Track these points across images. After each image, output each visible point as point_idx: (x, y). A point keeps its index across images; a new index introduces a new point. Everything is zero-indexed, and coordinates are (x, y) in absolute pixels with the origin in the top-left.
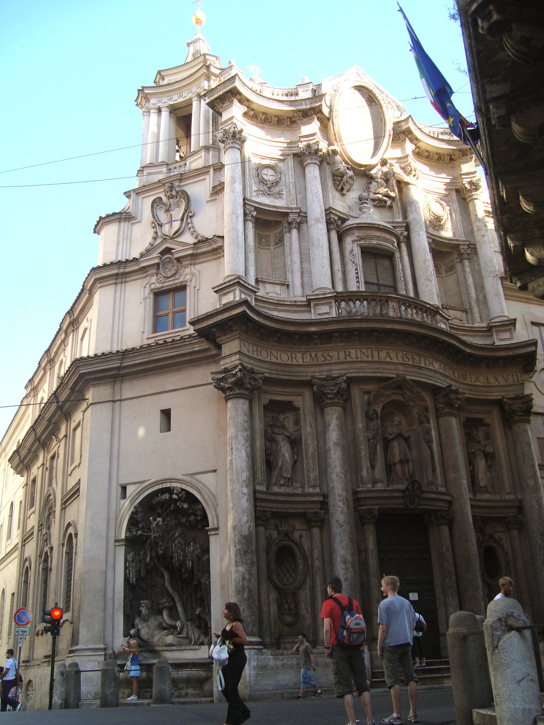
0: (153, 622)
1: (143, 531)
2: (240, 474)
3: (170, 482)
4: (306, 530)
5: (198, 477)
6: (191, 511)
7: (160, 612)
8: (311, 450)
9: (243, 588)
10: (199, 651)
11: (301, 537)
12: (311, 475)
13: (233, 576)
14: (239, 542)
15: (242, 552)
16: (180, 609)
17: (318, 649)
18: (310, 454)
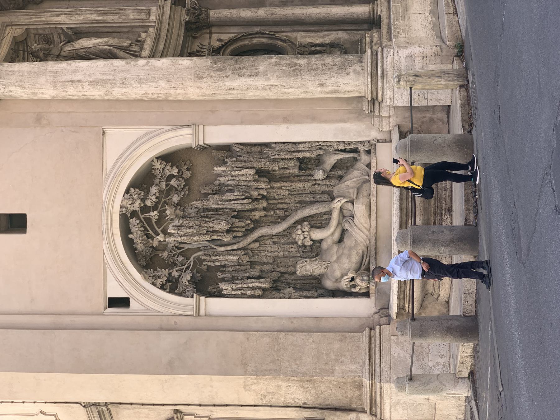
2: (116, 68)
4: (211, 34)
8: (94, 17)
9: (291, 65)
11: (220, 40)
12: (131, 17)
13: (273, 82)
14: (221, 70)
15: (237, 66)
17: (381, 11)
18: (100, 18)
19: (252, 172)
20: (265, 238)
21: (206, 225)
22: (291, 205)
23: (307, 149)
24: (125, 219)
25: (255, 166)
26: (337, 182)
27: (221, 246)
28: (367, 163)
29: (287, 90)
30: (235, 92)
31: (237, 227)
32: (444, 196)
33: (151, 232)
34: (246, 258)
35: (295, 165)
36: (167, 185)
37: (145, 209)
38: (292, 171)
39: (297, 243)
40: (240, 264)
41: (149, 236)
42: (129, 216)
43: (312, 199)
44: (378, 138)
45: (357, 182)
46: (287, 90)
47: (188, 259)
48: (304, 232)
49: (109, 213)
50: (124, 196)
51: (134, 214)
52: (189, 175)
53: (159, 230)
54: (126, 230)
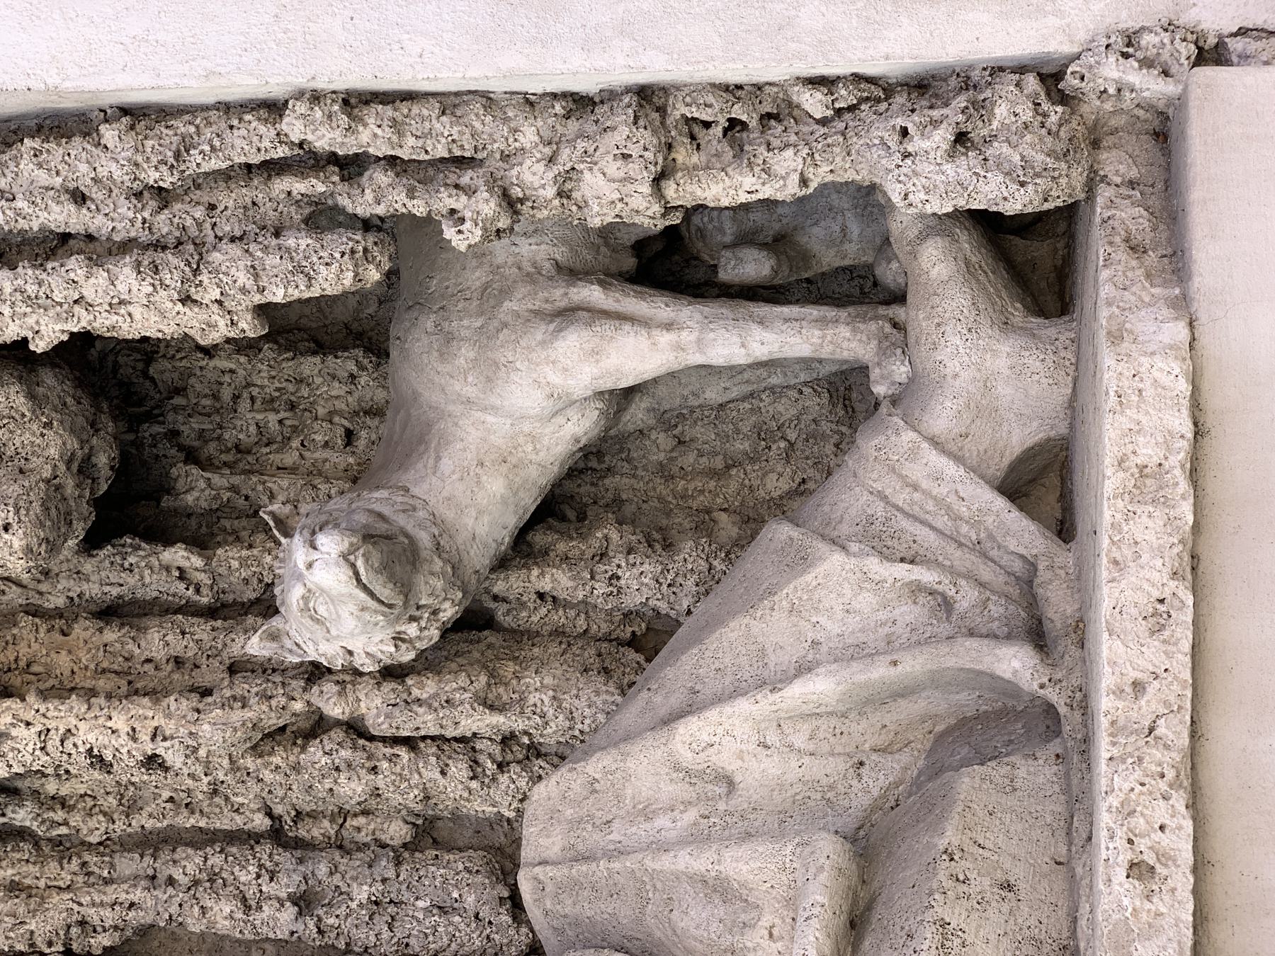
23: (118, 218)
26: (588, 700)
28: (1018, 437)
45: (865, 732)
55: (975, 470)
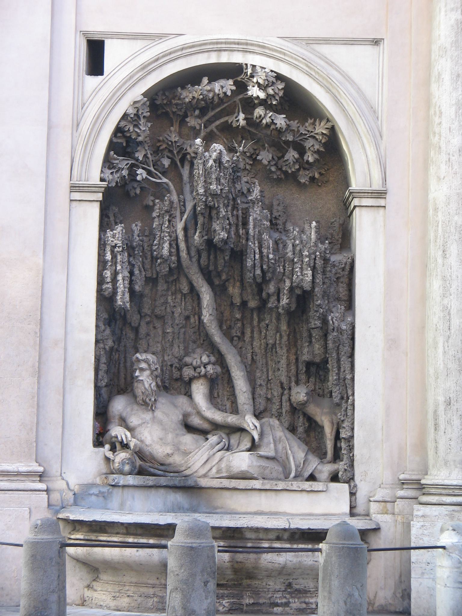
0: (169, 410)
1: (149, 173)
3: (245, 51)
5: (325, 49)
6: (290, 138)
7: (185, 387)
10: (322, 495)
16: (241, 384)
19: (307, 286)
20: (196, 302)
21: (221, 206)
22: (249, 348)
24: (234, 71)
25: (316, 289)
26: (286, 425)
27: (185, 229)
28: (317, 475)
29: (440, 345)
30: (440, 261)
31: (216, 257)
32: (261, 601)
33: (211, 114)
34: (165, 270)
35: (314, 356)
36: (287, 142)
37: (250, 104)
38: (306, 350)
39: (187, 354)
40: (154, 259)
41: (204, 111)
42: (239, 79)
43: (259, 382)
44: (358, 495)
46: (440, 345)
47: (164, 173)
48: (205, 368)
49: (245, 47)
50: (272, 71)
51: (242, 87)
52: (302, 181)
53: (213, 127)
54: (216, 72)
55: (313, 471)
